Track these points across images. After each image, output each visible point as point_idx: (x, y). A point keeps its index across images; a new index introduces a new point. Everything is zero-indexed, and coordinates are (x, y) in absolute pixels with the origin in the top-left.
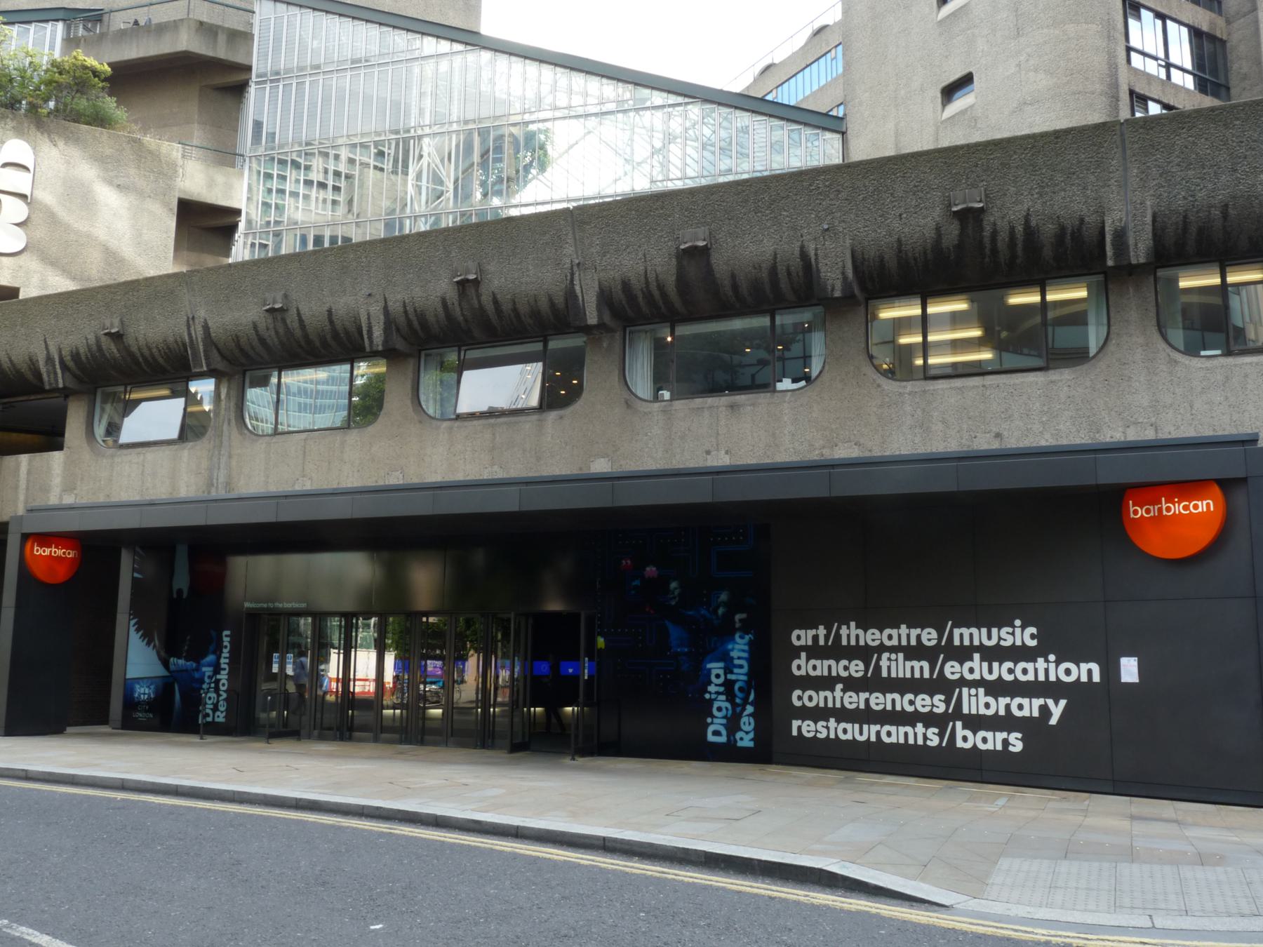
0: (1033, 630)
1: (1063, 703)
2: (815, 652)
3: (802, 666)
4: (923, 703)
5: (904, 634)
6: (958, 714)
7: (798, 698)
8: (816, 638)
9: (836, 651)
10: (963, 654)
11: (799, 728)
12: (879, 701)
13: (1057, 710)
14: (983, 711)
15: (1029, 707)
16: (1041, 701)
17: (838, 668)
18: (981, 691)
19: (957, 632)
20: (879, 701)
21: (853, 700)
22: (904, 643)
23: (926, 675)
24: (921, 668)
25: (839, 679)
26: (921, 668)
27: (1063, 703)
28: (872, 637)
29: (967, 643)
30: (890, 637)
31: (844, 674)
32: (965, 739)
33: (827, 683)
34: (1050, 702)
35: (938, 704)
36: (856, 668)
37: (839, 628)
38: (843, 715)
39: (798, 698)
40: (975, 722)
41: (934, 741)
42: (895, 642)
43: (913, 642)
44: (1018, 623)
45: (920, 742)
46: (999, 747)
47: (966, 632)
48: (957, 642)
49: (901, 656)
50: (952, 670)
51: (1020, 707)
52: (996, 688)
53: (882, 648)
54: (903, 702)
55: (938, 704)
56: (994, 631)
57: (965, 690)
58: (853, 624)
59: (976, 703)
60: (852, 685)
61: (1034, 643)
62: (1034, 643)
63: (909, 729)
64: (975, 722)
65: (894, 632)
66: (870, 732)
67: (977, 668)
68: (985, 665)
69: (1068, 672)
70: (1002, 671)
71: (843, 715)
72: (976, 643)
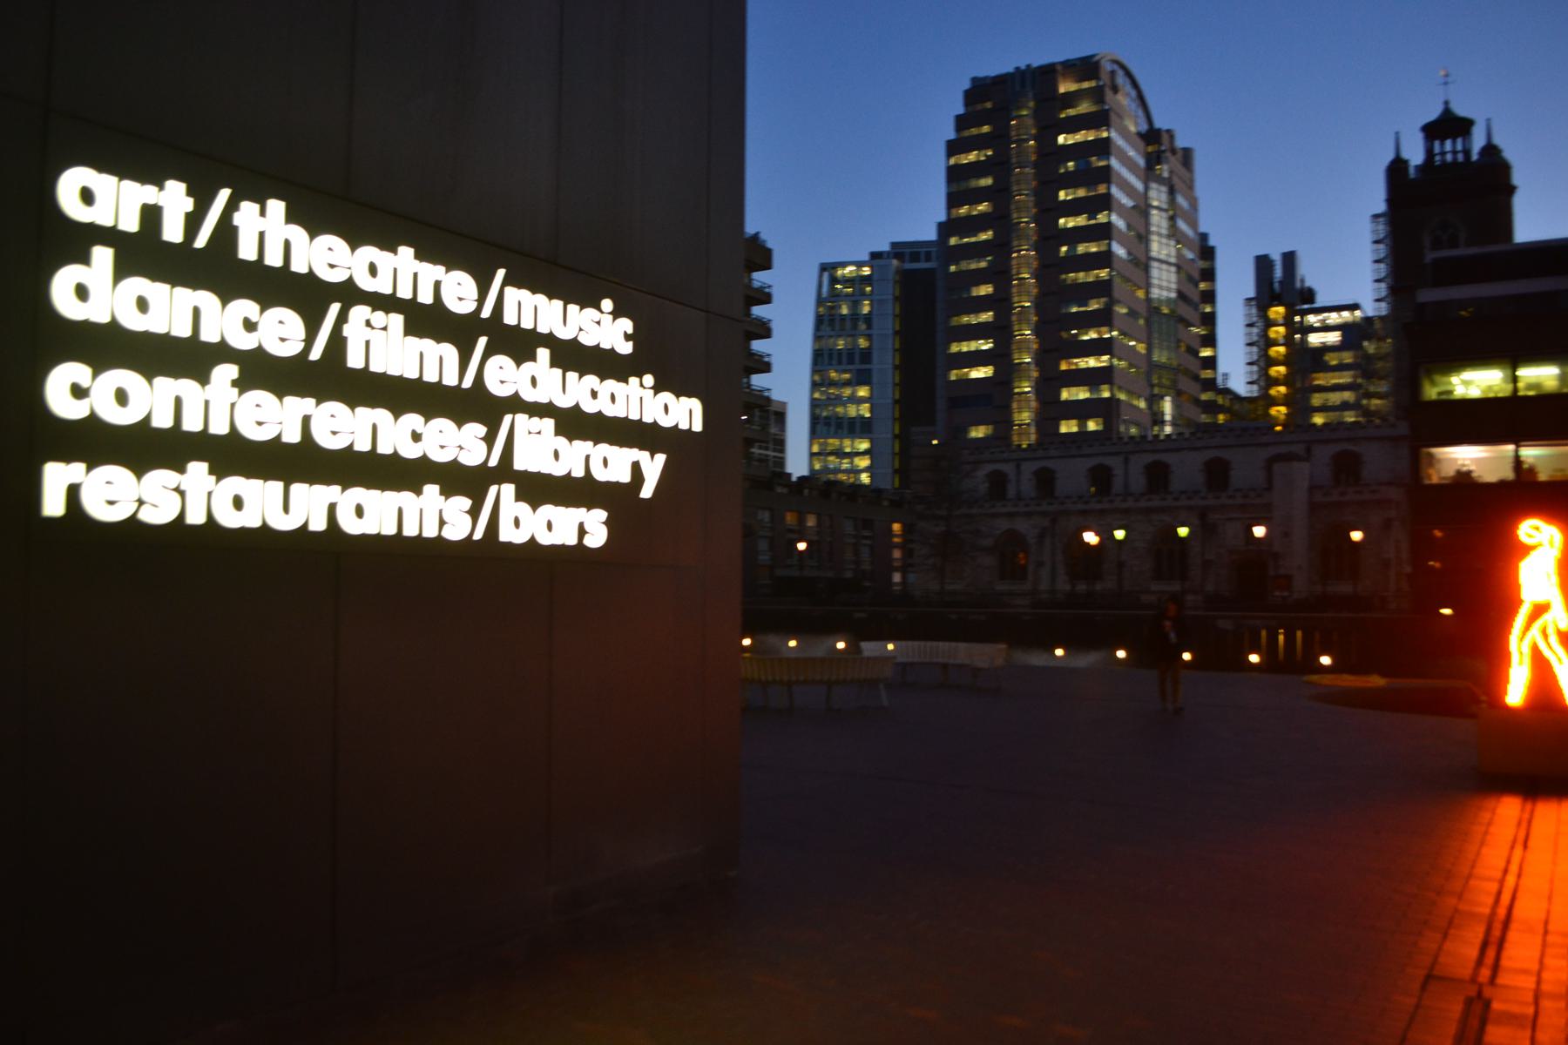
0: (626, 325)
2: (142, 253)
3: (88, 291)
5: (401, 269)
6: (504, 471)
7: (65, 390)
8: (152, 215)
9: (218, 268)
11: (73, 492)
12: (341, 426)
15: (614, 464)
17: (225, 320)
20: (341, 426)
21: (271, 417)
23: (451, 379)
24: (437, 361)
25: (222, 352)
26: (437, 361)
28: (325, 256)
31: (243, 342)
33: (187, 357)
35: (463, 443)
36: (281, 333)
37: (232, 206)
38: (233, 455)
39: (65, 390)
41: (458, 529)
44: (607, 304)
50: (503, 376)
52: (574, 424)
53: (349, 294)
54: (396, 434)
55: (463, 443)
58: (277, 207)
59: (539, 448)
60: (260, 371)
61: (626, 348)
66: (307, 506)
70: (580, 391)
71: (233, 455)
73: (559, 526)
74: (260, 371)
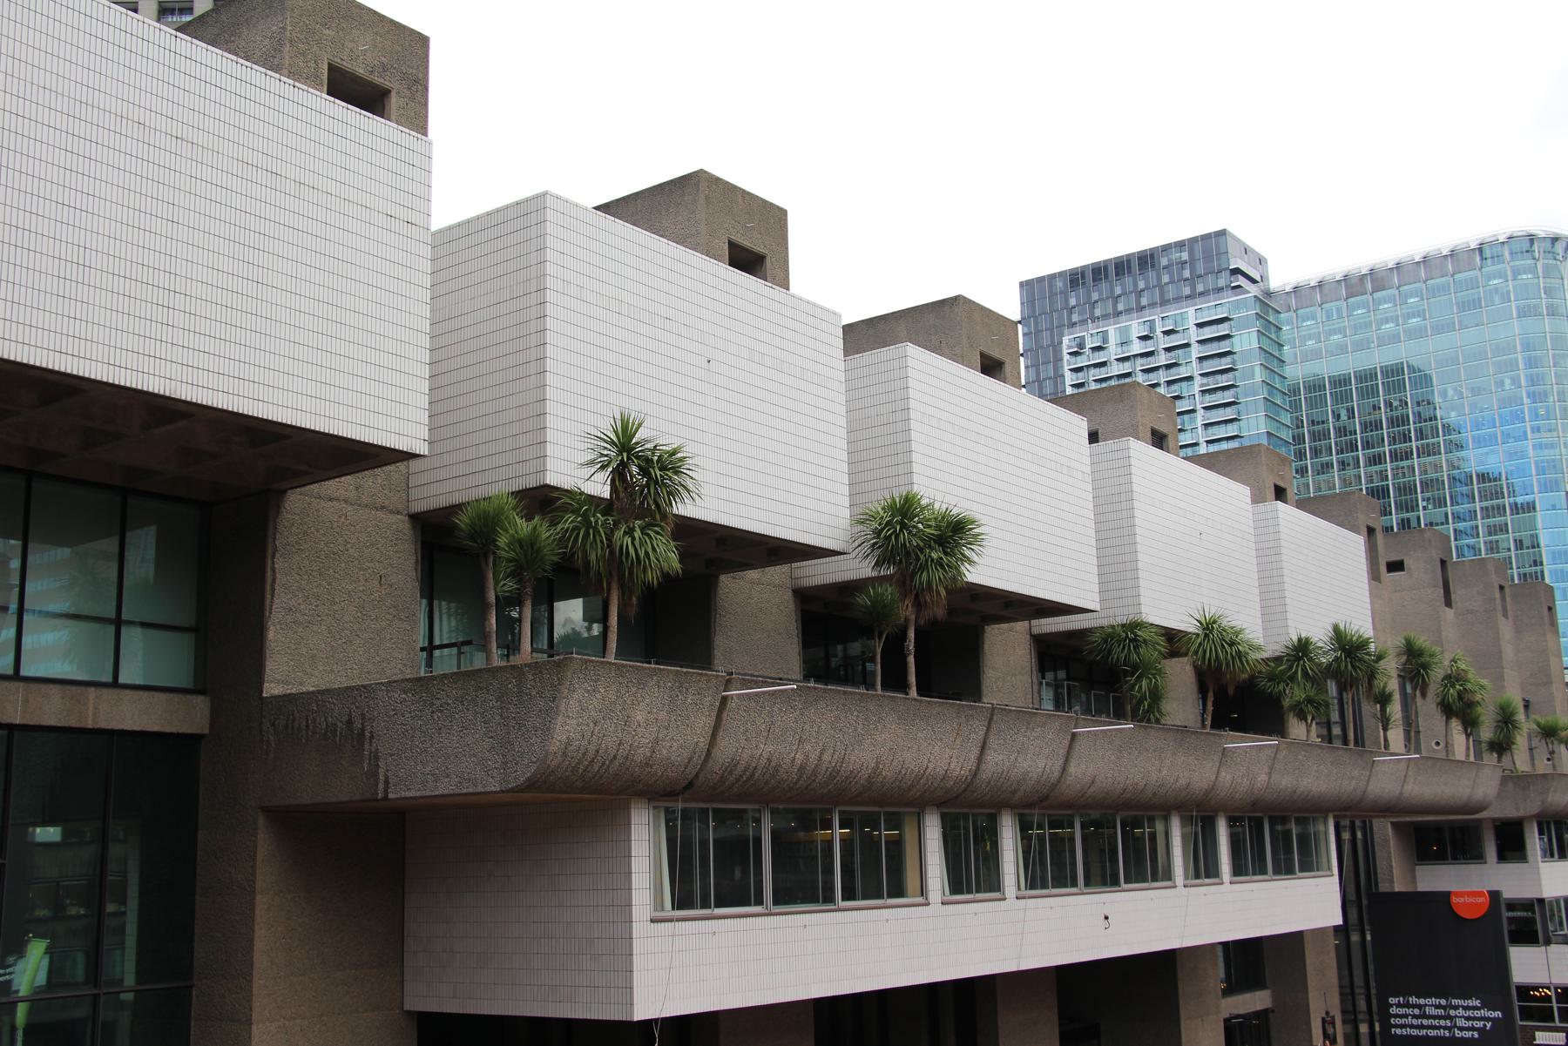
2: (1399, 1005)
3: (1393, 1010)
4: (1442, 1023)
9: (1408, 1005)
10: (1456, 1008)
12: (1425, 1022)
13: (1489, 1025)
15: (1480, 1024)
17: (1410, 1011)
20: (1425, 1022)
21: (1415, 1022)
24: (1441, 1012)
26: (1441, 1012)
28: (1422, 1001)
33: (1406, 1016)
36: (1417, 1011)
38: (1412, 1026)
40: (1461, 1029)
50: (1452, 1013)
52: (1468, 1019)
54: (1436, 1023)
59: (1461, 1023)
60: (1414, 1016)
64: (1461, 1029)
66: (1423, 1032)
67: (1461, 1012)
70: (1470, 1013)
71: (1412, 1026)
73: (1468, 1034)
74: (1414, 1016)
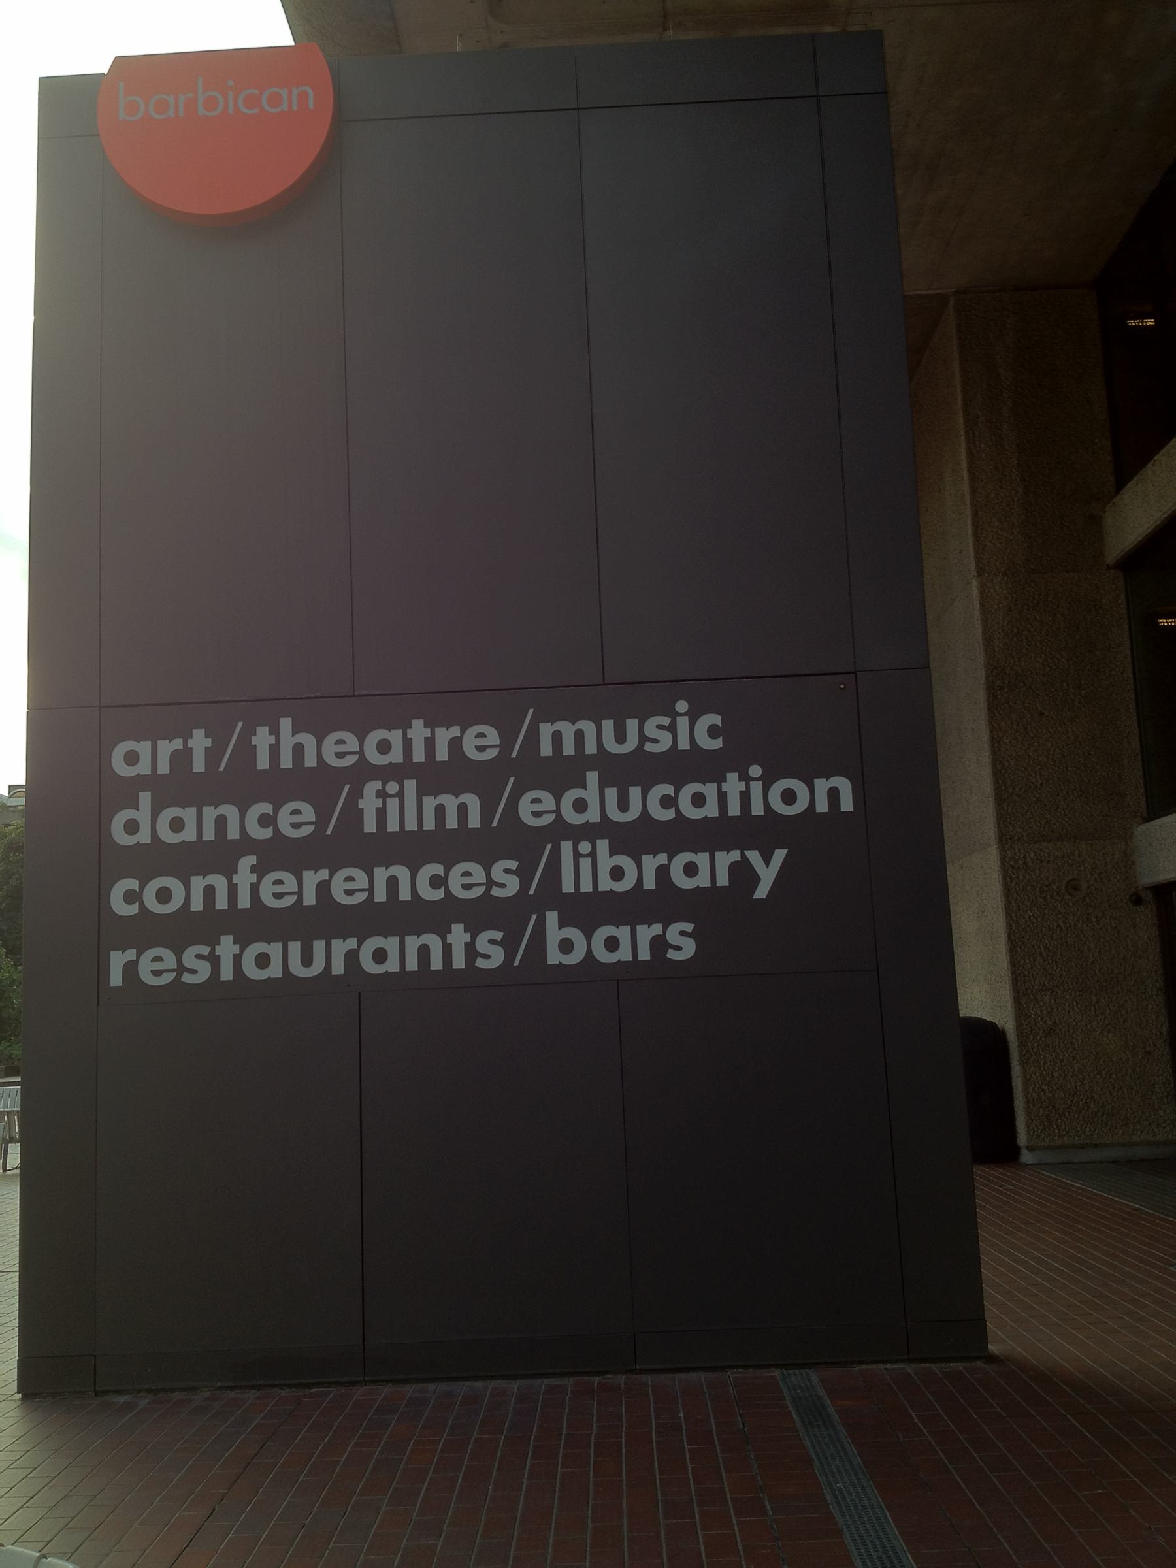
0: (715, 719)
1: (780, 855)
4: (466, 879)
6: (551, 894)
10: (562, 774)
14: (606, 884)
16: (735, 855)
18: (603, 845)
19: (546, 731)
22: (419, 756)
24: (462, 808)
27: (780, 855)
29: (569, 749)
30: (384, 747)
32: (566, 946)
34: (754, 856)
40: (588, 911)
42: (396, 756)
43: (442, 755)
44: (682, 706)
45: (459, 962)
46: (644, 954)
47: (567, 730)
48: (546, 750)
49: (411, 786)
50: (537, 806)
51: (691, 870)
53: (363, 771)
54: (419, 883)
56: (632, 725)
57: (566, 847)
61: (717, 744)
62: (717, 744)
63: (433, 941)
64: (588, 911)
65: (395, 737)
68: (611, 793)
69: (789, 797)
70: (651, 802)
72: (591, 748)
